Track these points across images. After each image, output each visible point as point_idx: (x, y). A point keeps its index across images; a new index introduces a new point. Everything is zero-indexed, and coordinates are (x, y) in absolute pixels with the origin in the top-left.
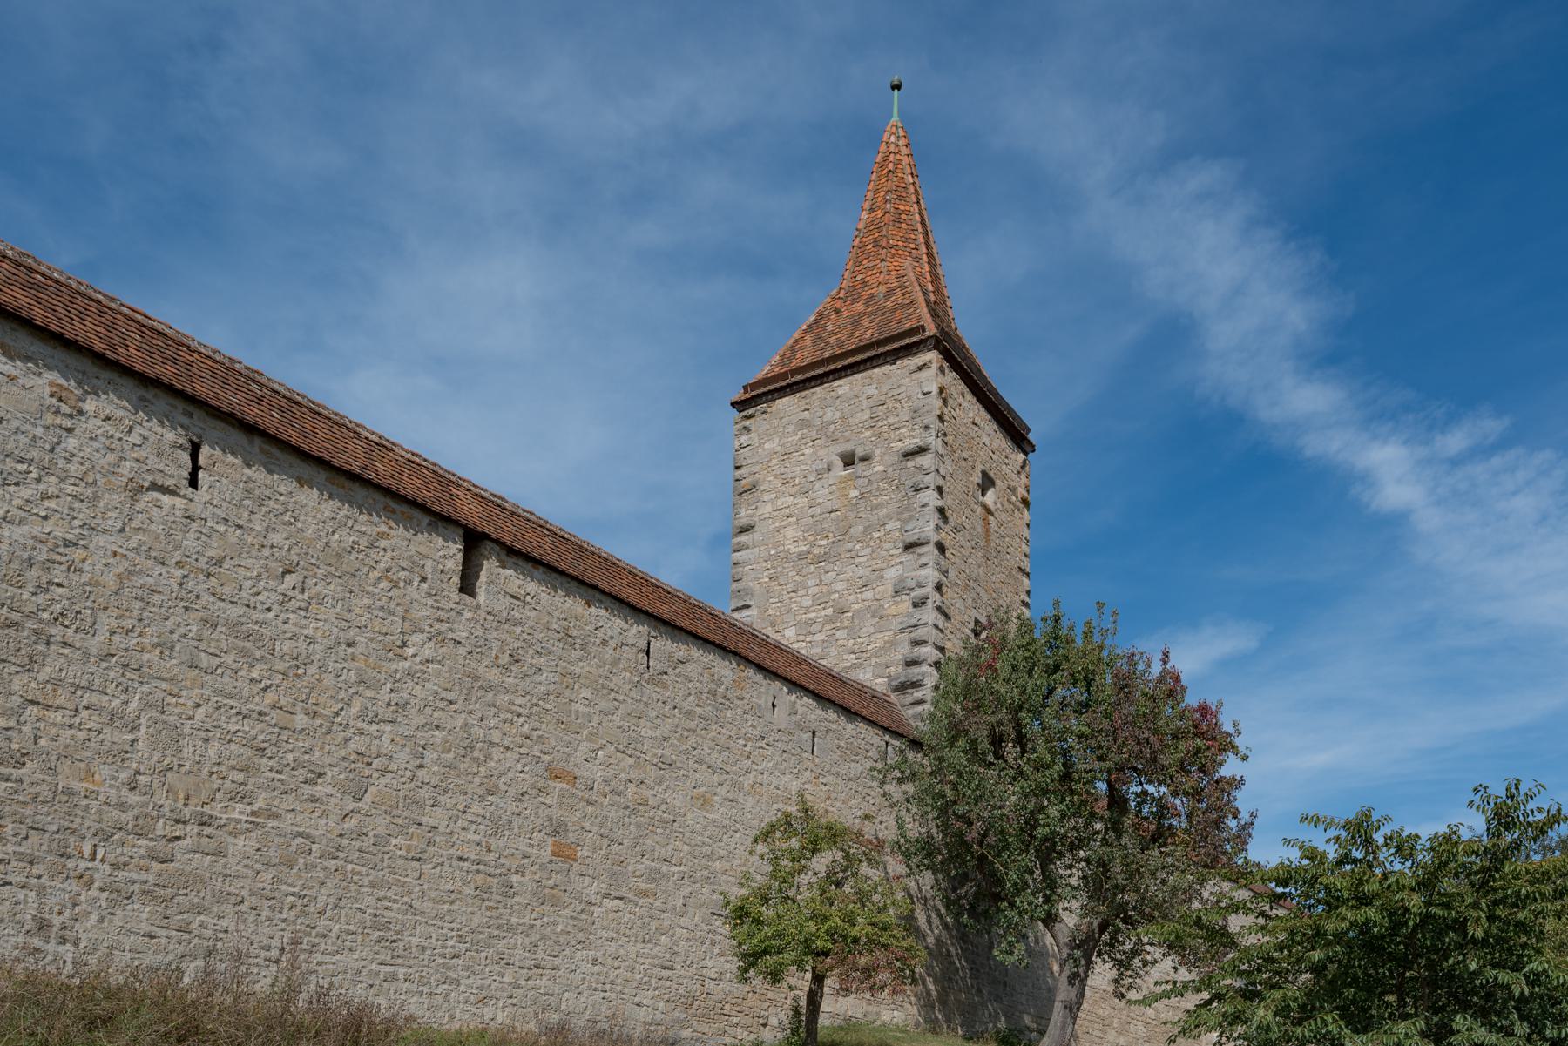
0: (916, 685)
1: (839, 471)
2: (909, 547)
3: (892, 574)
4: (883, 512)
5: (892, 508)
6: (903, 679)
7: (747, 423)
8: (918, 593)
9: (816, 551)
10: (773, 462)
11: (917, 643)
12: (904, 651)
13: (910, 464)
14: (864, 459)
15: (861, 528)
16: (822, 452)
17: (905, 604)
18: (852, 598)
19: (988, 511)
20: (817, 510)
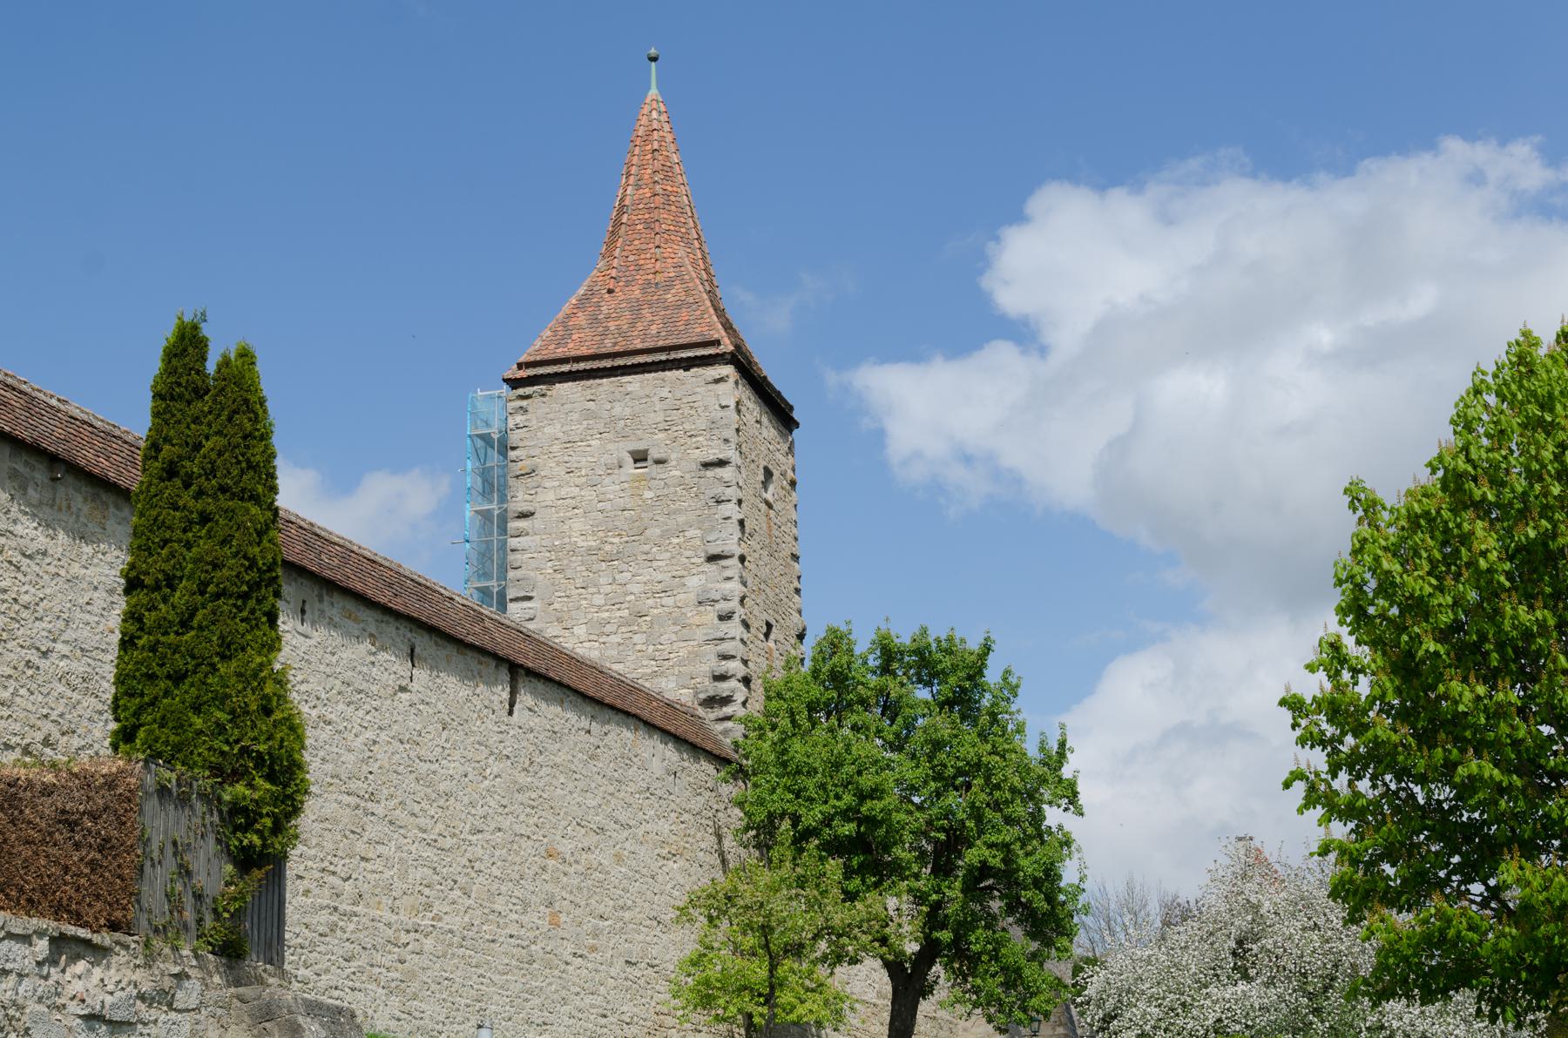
0: (726, 701)
1: (630, 468)
2: (712, 558)
3: (694, 582)
4: (681, 519)
5: (692, 516)
6: (711, 693)
7: (524, 403)
8: (724, 607)
9: (608, 547)
10: (555, 448)
11: (725, 657)
12: (712, 664)
13: (710, 473)
14: (659, 462)
15: (658, 531)
16: (610, 446)
17: (710, 615)
18: (650, 602)
19: (770, 506)
20: (607, 505)
